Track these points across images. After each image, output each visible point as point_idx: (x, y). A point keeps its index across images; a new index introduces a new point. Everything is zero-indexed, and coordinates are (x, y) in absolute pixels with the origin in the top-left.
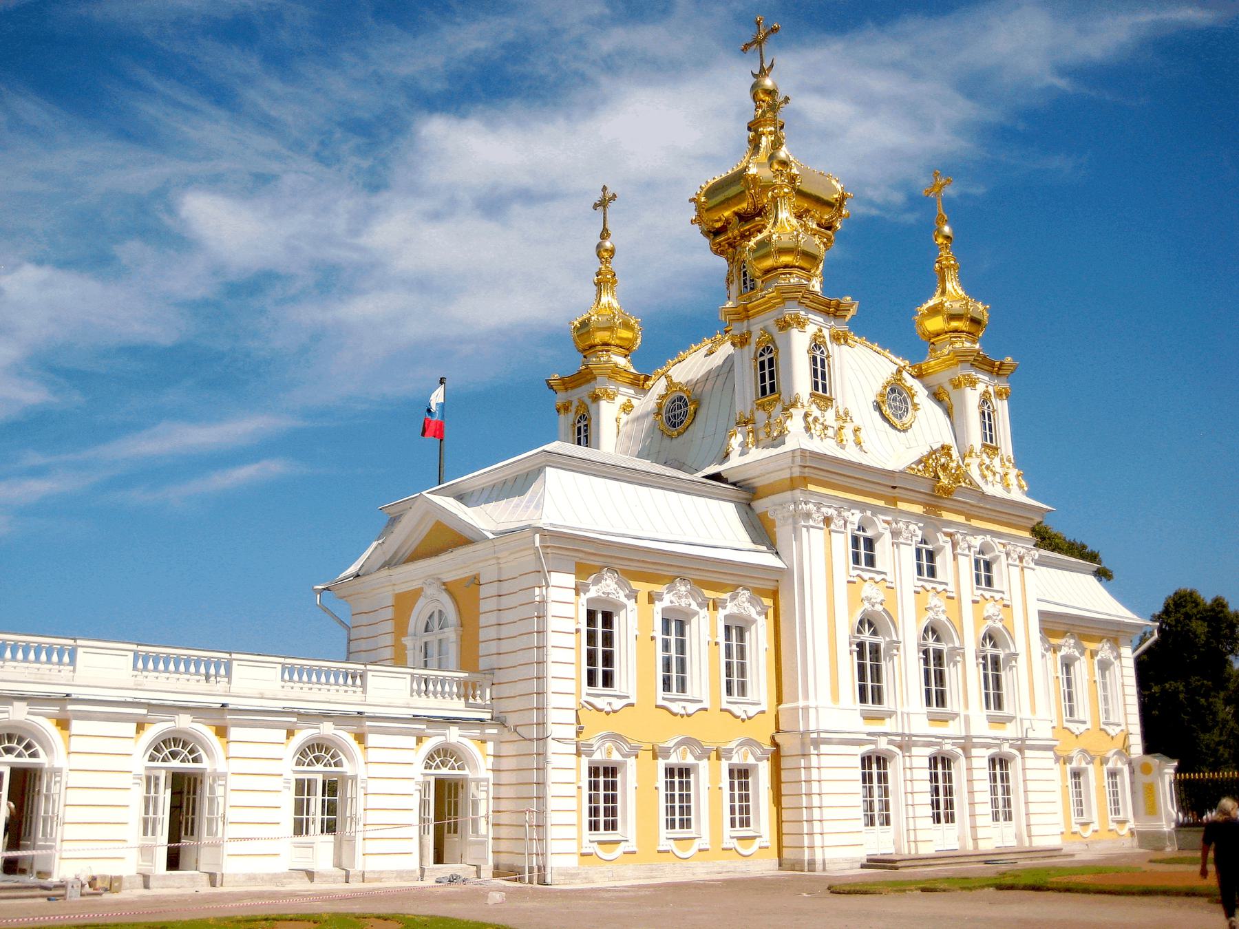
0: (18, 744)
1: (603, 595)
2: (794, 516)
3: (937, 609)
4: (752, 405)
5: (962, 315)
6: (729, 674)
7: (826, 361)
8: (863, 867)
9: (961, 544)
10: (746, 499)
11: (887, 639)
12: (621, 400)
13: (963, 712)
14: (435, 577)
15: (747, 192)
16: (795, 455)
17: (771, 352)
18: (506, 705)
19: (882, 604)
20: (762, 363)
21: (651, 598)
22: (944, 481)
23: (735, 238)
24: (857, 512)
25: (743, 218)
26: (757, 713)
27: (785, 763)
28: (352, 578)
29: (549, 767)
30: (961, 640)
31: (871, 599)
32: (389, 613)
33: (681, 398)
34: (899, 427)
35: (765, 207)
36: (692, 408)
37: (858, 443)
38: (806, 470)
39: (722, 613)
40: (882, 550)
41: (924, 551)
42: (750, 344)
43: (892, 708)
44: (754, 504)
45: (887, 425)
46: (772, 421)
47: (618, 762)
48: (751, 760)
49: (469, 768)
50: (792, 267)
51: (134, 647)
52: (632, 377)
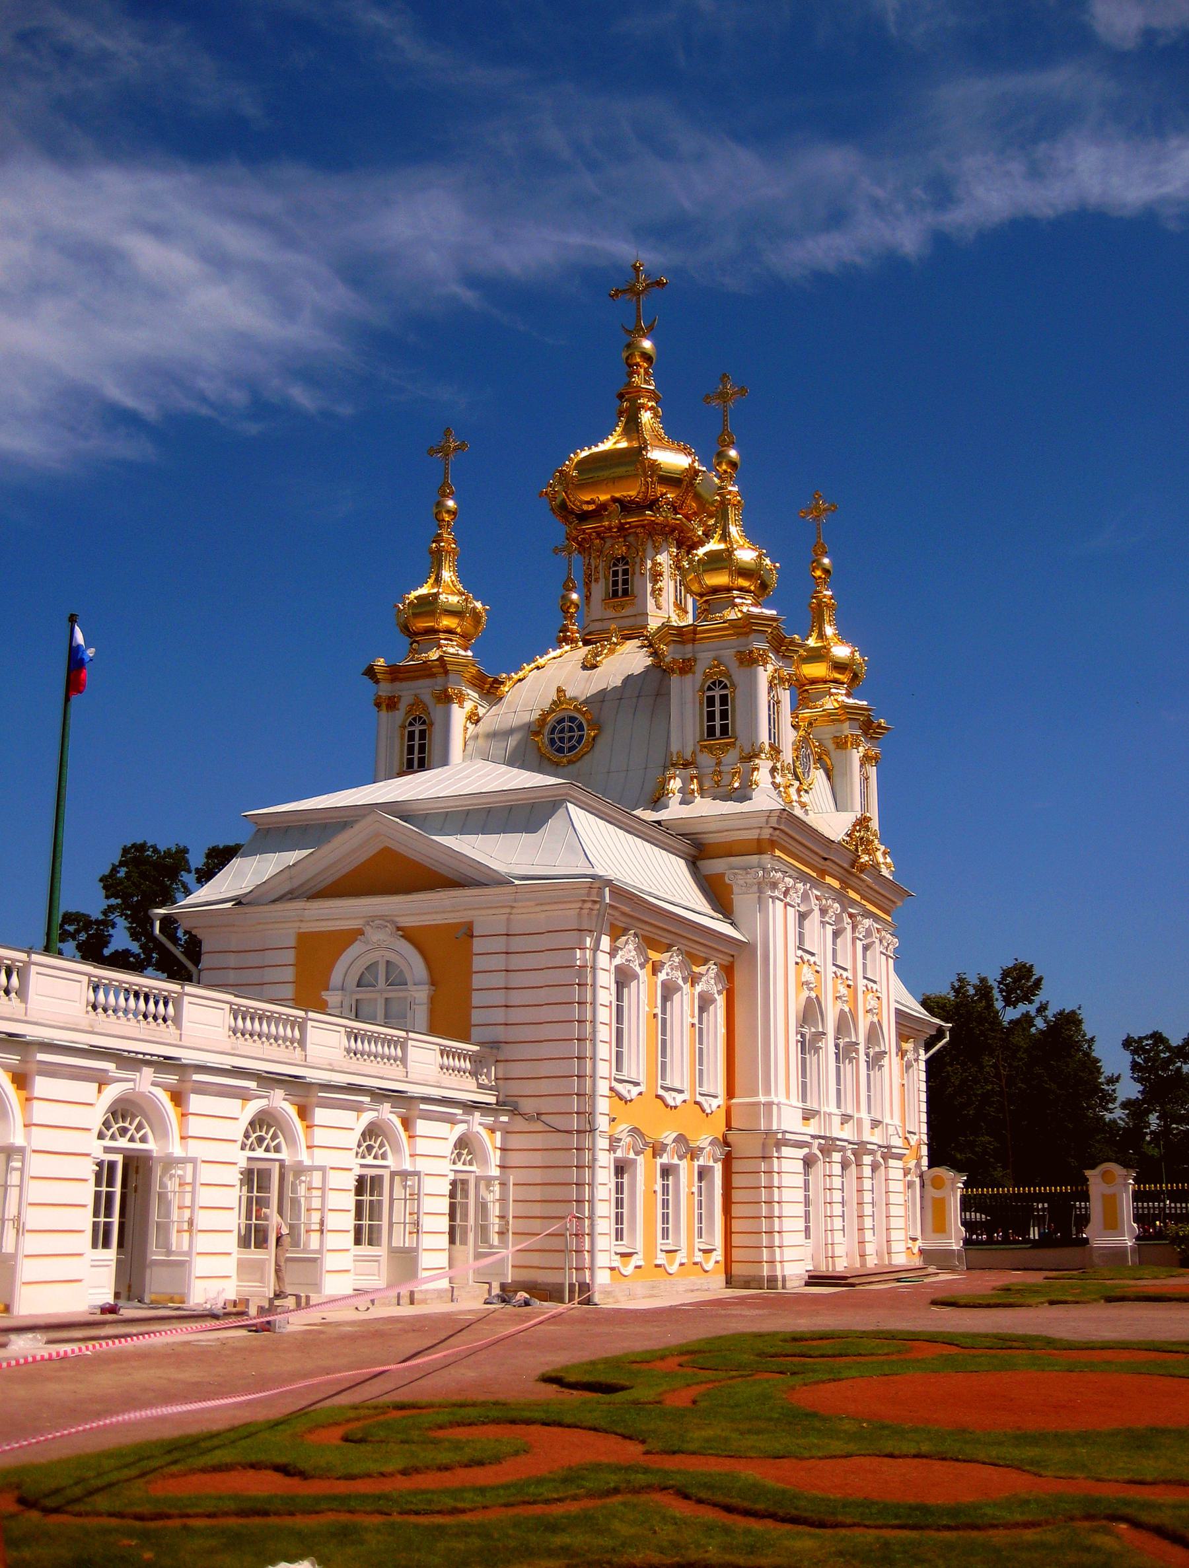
2: (759, 884)
4: (694, 745)
8: (807, 1284)
10: (694, 857)
11: (813, 1030)
12: (469, 705)
14: (388, 918)
17: (725, 687)
18: (515, 1088)
25: (627, 506)
27: (737, 1166)
32: (290, 957)
33: (572, 719)
35: (658, 500)
38: (777, 832)
42: (694, 673)
44: (700, 863)
46: (723, 768)
48: (711, 1163)
50: (747, 592)
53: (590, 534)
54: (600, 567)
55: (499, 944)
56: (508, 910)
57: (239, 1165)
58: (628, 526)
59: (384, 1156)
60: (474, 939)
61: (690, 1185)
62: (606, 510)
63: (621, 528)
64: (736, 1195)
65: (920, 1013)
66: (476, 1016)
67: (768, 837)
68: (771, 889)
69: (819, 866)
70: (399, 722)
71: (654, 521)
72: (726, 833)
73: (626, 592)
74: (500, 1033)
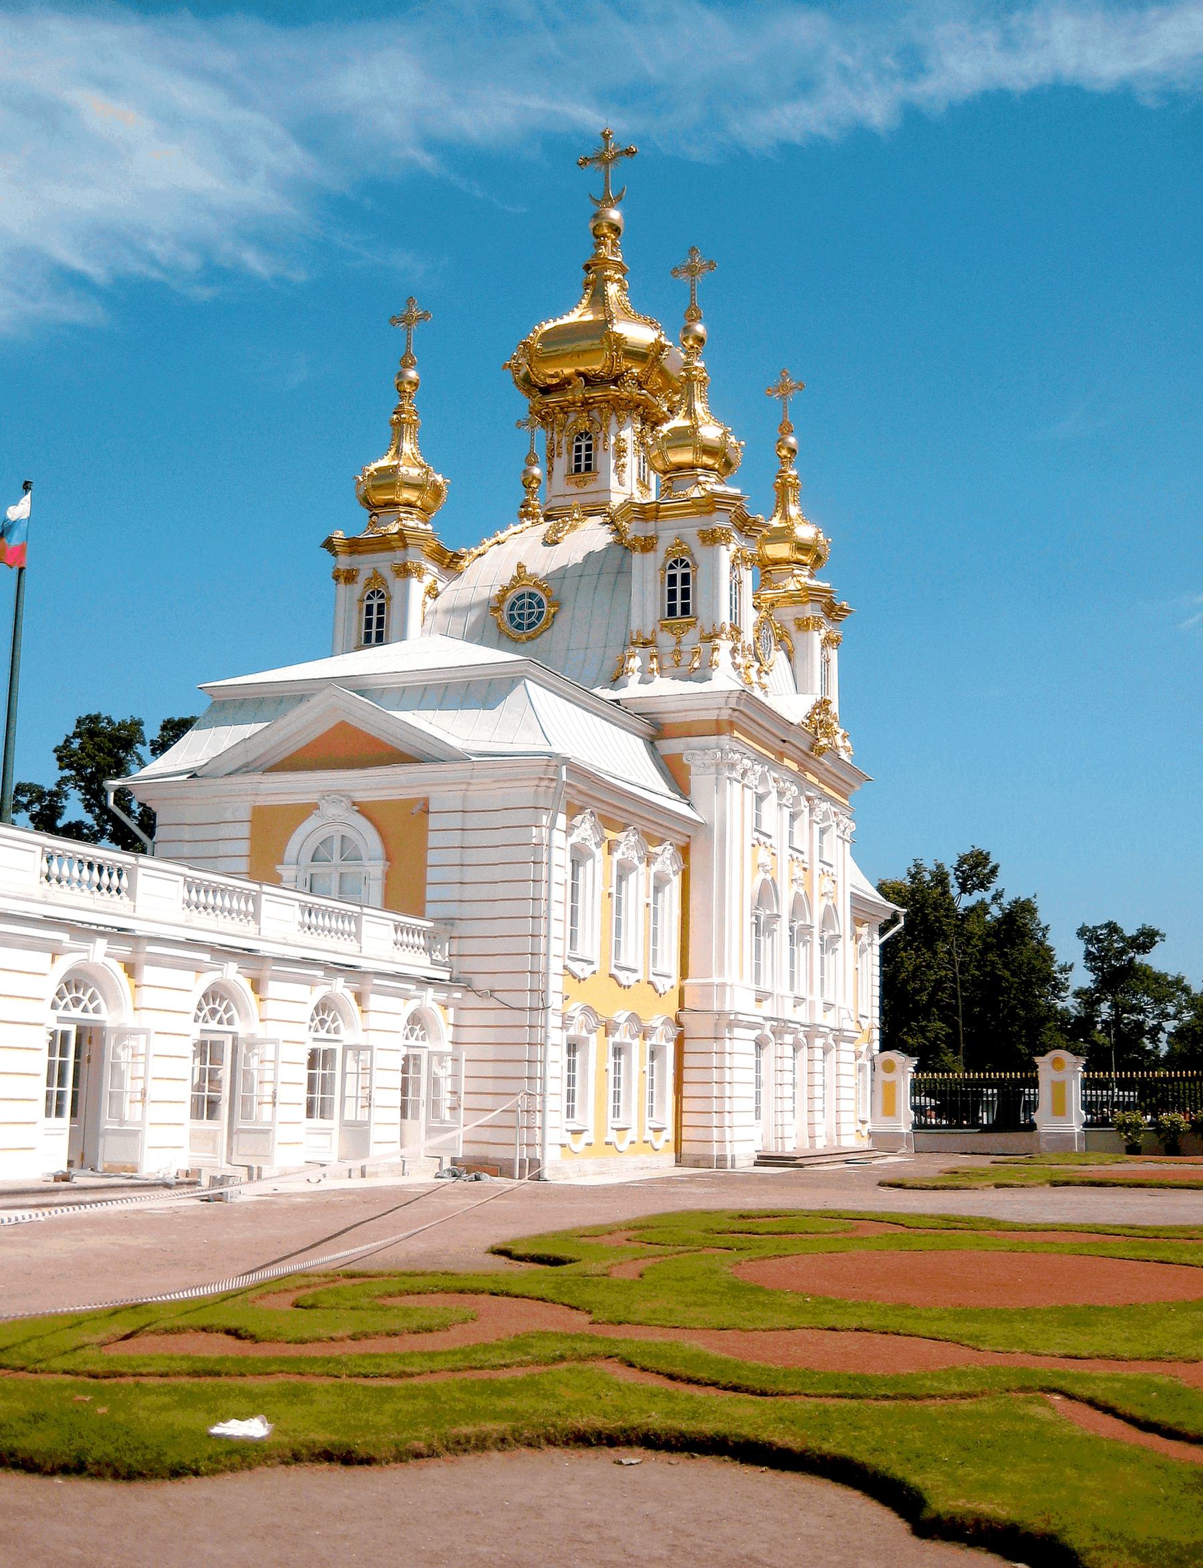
2: (717, 765)
4: (655, 624)
8: (756, 1164)
10: (652, 736)
11: (768, 912)
12: (428, 580)
13: (809, 998)
14: (343, 793)
17: (687, 566)
18: (469, 964)
25: (590, 380)
27: (689, 1046)
29: (550, 1042)
32: (244, 830)
33: (531, 595)
35: (623, 375)
38: (737, 713)
42: (656, 551)
48: (663, 1043)
51: (185, 871)
53: (553, 409)
54: (563, 442)
55: (456, 821)
56: (464, 787)
58: (591, 401)
59: (337, 1030)
61: (642, 1063)
62: (569, 384)
63: (585, 403)
64: (688, 1075)
65: (875, 897)
66: (431, 893)
67: (726, 718)
68: (729, 770)
69: (777, 748)
72: (684, 713)
74: (453, 910)
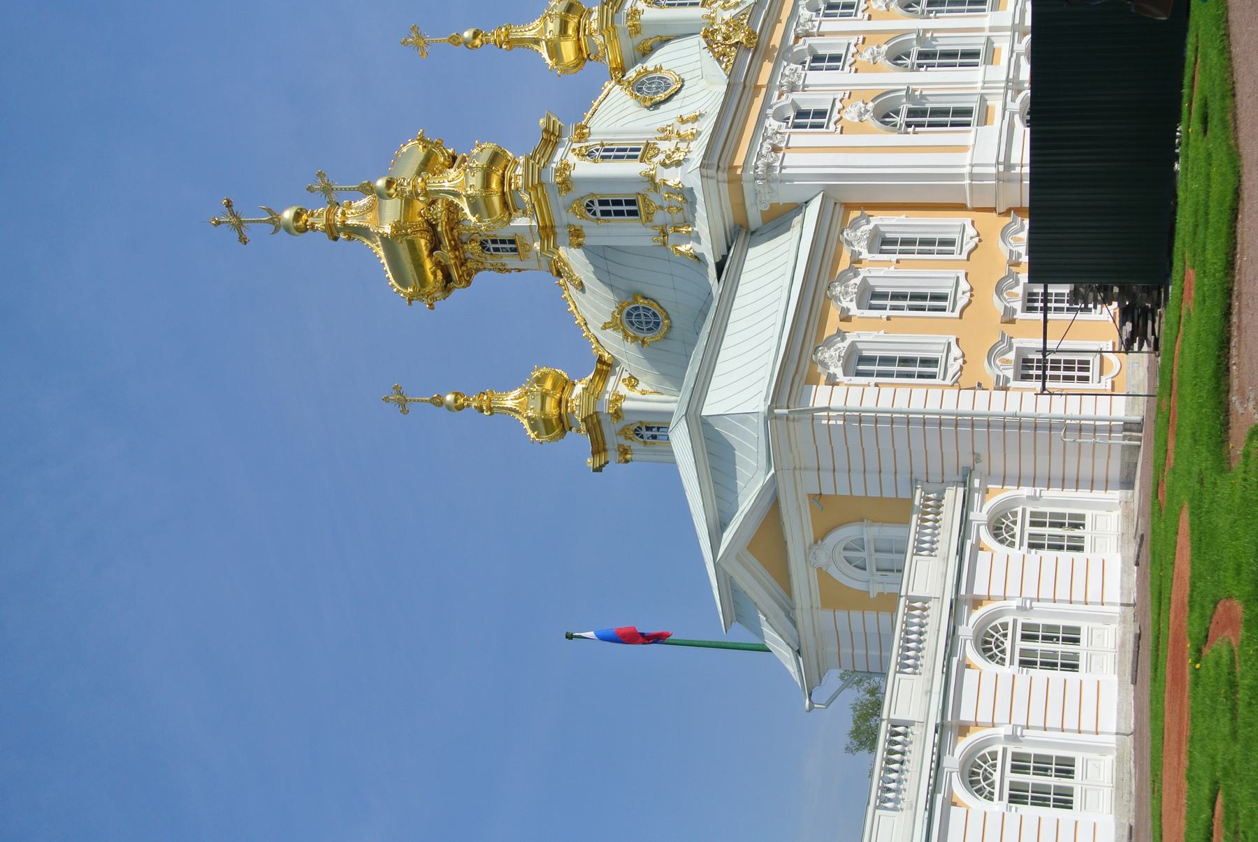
0: (978, 774)
1: (841, 362)
3: (875, 52)
5: (561, 21)
6: (922, 309)
7: (606, 147)
9: (808, 28)
11: (904, 100)
12: (623, 390)
14: (807, 551)
15: (409, 238)
16: (706, 175)
17: (592, 202)
19: (866, 104)
20: (604, 213)
21: (845, 317)
22: (741, 37)
23: (456, 257)
24: (767, 123)
25: (435, 245)
26: (974, 227)
28: (801, 659)
29: (1019, 413)
30: (909, 32)
31: (861, 113)
32: (842, 615)
34: (679, 86)
36: (641, 301)
37: (695, 119)
38: (721, 165)
39: (865, 255)
40: (808, 101)
41: (812, 64)
42: (582, 227)
43: (977, 98)
44: (752, 228)
45: (675, 97)
46: (666, 204)
47: (1017, 355)
49: (1015, 508)
50: (503, 177)
51: (871, 808)
52: (597, 379)
56: (797, 472)
57: (1005, 811)
59: (1005, 626)
60: (823, 493)
62: (440, 262)
66: (889, 493)
67: (726, 175)
69: (751, 92)
70: (641, 447)
71: (446, 223)
72: (724, 210)
73: (512, 242)
74: (903, 477)
